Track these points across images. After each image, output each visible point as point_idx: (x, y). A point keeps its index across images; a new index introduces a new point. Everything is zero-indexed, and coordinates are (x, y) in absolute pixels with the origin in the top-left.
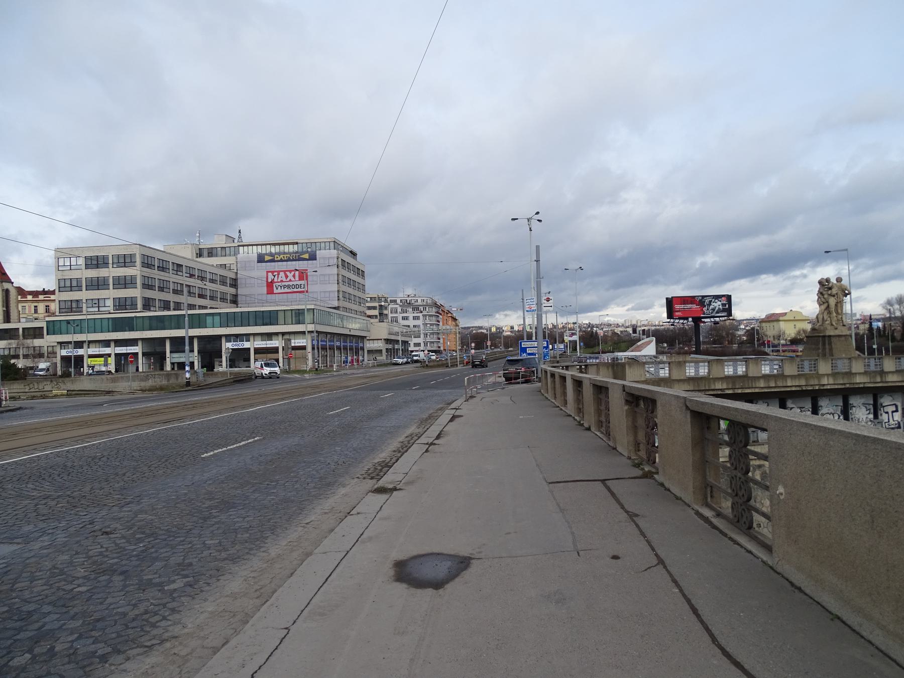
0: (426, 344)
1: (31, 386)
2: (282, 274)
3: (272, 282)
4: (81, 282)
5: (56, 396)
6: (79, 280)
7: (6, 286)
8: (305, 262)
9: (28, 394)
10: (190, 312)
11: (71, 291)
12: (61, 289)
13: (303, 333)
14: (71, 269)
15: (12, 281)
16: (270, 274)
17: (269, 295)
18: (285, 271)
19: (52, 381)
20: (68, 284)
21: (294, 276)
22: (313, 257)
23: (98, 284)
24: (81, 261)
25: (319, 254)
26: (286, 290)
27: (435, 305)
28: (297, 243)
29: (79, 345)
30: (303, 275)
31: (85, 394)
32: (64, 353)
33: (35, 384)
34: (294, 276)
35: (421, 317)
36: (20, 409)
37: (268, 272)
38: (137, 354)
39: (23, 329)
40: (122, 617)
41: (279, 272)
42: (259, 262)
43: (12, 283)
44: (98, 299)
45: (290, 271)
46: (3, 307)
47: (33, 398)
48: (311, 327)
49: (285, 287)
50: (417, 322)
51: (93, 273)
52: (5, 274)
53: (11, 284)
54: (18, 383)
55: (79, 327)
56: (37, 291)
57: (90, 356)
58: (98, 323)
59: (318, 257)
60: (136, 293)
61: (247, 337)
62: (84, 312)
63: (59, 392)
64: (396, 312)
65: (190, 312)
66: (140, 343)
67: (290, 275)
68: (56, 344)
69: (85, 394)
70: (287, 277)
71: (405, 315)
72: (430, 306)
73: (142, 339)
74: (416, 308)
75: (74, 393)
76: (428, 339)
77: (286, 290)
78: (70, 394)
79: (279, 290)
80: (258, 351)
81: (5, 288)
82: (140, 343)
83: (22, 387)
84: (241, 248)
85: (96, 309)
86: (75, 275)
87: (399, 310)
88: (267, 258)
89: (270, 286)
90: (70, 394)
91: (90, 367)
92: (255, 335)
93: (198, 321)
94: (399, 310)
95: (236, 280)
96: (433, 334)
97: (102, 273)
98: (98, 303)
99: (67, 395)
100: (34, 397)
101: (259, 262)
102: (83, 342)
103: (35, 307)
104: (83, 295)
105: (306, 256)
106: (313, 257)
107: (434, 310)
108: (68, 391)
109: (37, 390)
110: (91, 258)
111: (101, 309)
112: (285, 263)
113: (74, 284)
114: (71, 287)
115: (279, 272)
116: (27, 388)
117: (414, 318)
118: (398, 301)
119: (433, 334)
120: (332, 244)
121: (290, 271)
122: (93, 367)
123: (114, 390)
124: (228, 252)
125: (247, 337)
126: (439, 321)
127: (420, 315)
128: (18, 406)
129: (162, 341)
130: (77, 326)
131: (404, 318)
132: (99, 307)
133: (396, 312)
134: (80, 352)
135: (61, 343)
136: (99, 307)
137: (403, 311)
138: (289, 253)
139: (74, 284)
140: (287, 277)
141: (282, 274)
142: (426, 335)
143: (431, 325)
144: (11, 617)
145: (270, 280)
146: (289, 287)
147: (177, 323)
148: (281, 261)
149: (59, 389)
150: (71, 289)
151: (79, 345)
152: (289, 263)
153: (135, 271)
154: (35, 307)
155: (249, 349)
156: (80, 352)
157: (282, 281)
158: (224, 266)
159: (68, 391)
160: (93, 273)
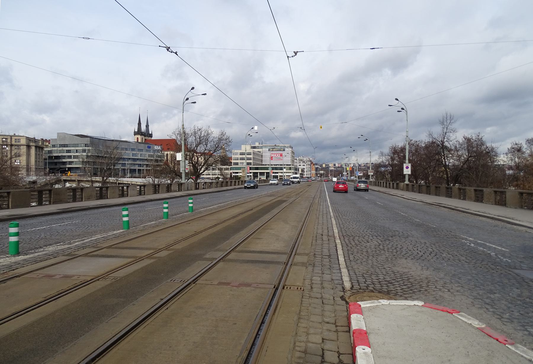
0: (307, 174)
2: (275, 155)
3: (273, 156)
6: (238, 158)
8: (282, 151)
10: (271, 166)
13: (291, 172)
16: (272, 154)
17: (271, 160)
18: (276, 154)
20: (235, 159)
21: (279, 155)
22: (284, 150)
23: (242, 159)
25: (286, 149)
26: (276, 159)
27: (311, 161)
28: (279, 146)
30: (281, 155)
34: (279, 155)
35: (306, 165)
37: (271, 154)
38: (251, 176)
41: (274, 154)
42: (269, 151)
45: (278, 154)
48: (293, 171)
49: (277, 158)
50: (304, 167)
55: (237, 169)
59: (285, 150)
60: (251, 161)
61: (278, 173)
64: (297, 163)
65: (271, 166)
66: (252, 173)
67: (278, 155)
70: (276, 155)
71: (300, 164)
72: (309, 161)
73: (253, 172)
74: (304, 162)
76: (307, 173)
77: (276, 159)
79: (274, 159)
80: (280, 176)
82: (252, 173)
84: (263, 147)
87: (298, 162)
88: (271, 150)
89: (272, 158)
92: (279, 172)
93: (267, 169)
94: (298, 162)
95: (262, 156)
96: (309, 171)
97: (244, 156)
98: (242, 163)
101: (269, 151)
104: (239, 161)
105: (282, 150)
106: (284, 150)
107: (310, 163)
110: (241, 153)
112: (276, 152)
113: (237, 159)
115: (274, 154)
117: (303, 165)
118: (298, 159)
119: (309, 171)
120: (289, 147)
121: (278, 154)
124: (259, 148)
125: (278, 173)
126: (311, 167)
127: (305, 164)
129: (257, 173)
131: (299, 165)
133: (297, 163)
134: (237, 174)
137: (299, 163)
138: (278, 149)
140: (276, 155)
141: (275, 155)
142: (307, 172)
143: (309, 168)
145: (272, 156)
146: (277, 158)
147: (262, 169)
148: (275, 151)
150: (236, 160)
152: (277, 151)
153: (251, 156)
155: (278, 176)
156: (237, 174)
157: (275, 157)
158: (258, 151)
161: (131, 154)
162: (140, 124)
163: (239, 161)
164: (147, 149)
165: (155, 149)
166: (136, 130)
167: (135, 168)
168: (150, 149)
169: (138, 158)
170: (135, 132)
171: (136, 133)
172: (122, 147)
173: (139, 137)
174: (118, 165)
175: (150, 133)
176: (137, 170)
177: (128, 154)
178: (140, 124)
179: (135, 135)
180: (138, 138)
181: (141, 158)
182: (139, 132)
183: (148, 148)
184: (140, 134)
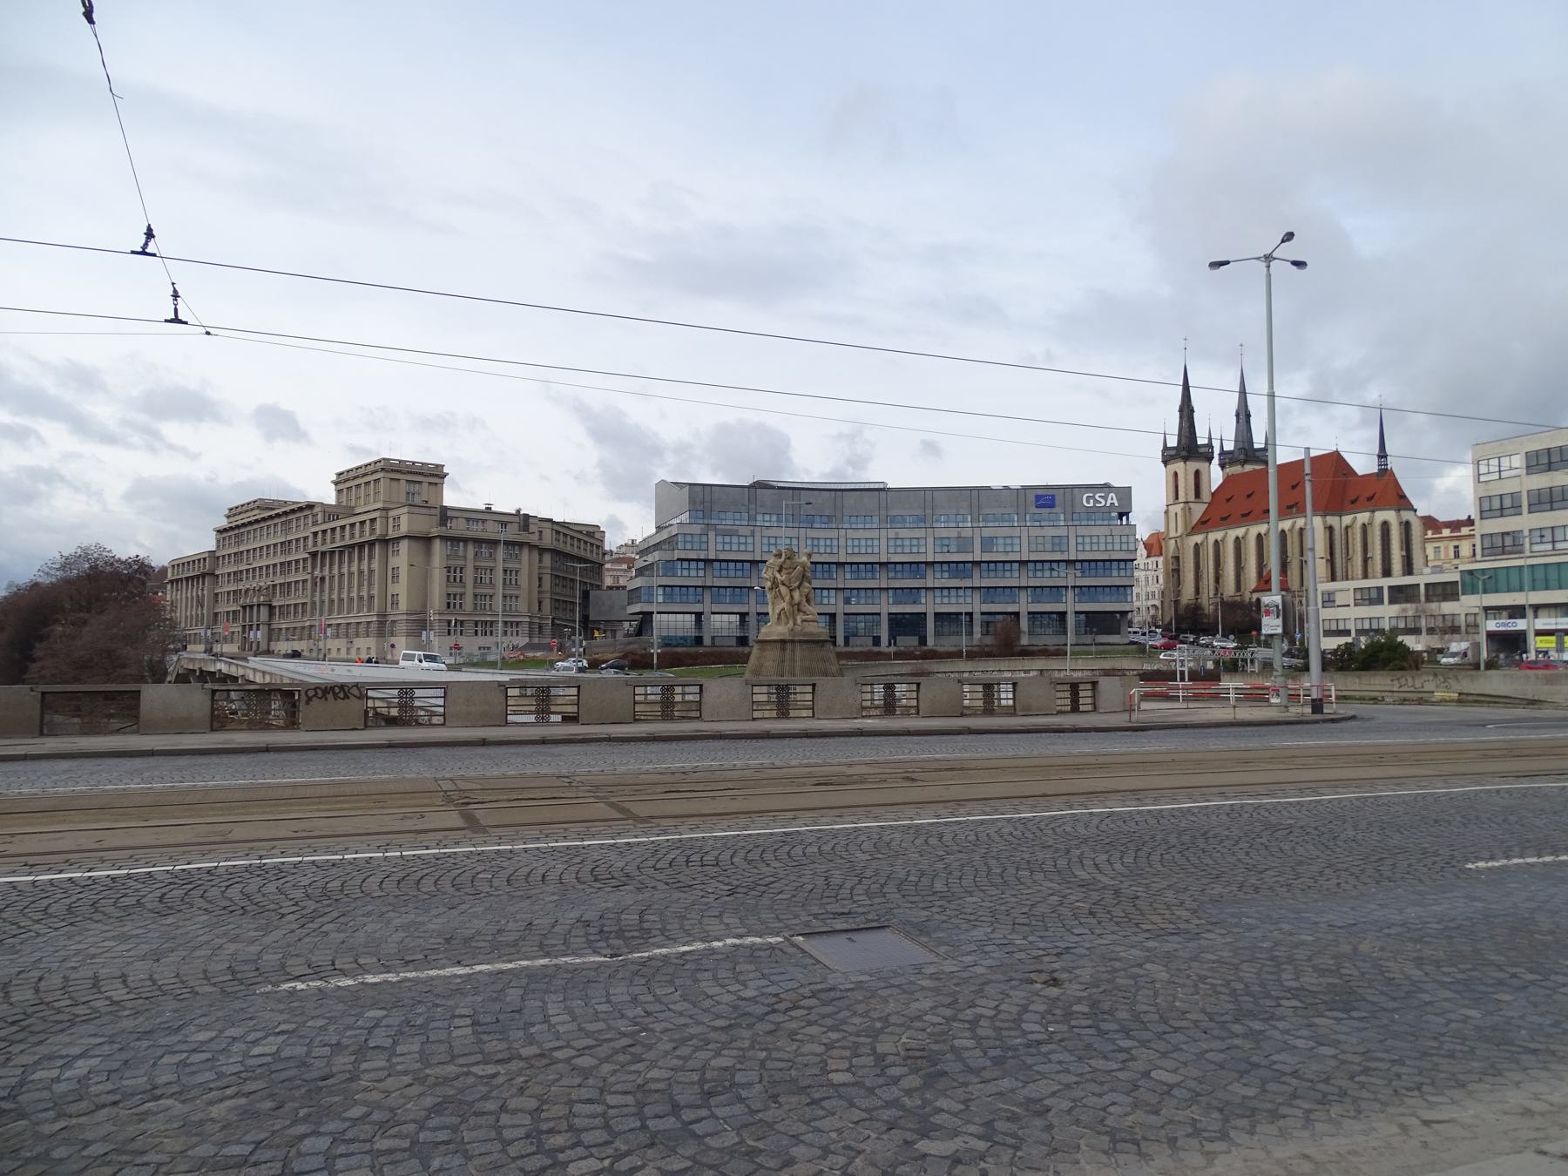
1: (1403, 681)
4: (1520, 498)
5: (1442, 702)
7: (1406, 515)
9: (1395, 694)
11: (1502, 516)
12: (1485, 515)
14: (1500, 478)
15: (1415, 507)
19: (1436, 675)
20: (1496, 504)
24: (1518, 461)
29: (1517, 612)
31: (1490, 702)
32: (1492, 625)
33: (1410, 680)
36: (1353, 718)
39: (1427, 585)
40: (1248, 1113)
43: (1416, 511)
44: (1553, 528)
46: (1402, 549)
47: (1404, 701)
51: (1541, 481)
52: (1403, 497)
53: (1412, 513)
54: (1382, 675)
56: (1458, 521)
57: (1539, 633)
58: (1502, 576)
62: (1528, 553)
63: (1447, 695)
68: (1476, 611)
69: (1490, 702)
75: (1470, 698)
78: (1463, 699)
81: (1404, 519)
83: (1389, 682)
85: (1549, 547)
86: (1509, 487)
90: (1463, 699)
91: (1541, 652)
99: (1459, 701)
100: (1405, 700)
102: (1523, 608)
103: (1456, 547)
104: (1524, 522)
108: (1460, 694)
109: (1412, 689)
111: (1559, 546)
113: (1507, 502)
114: (1502, 509)
116: (1396, 682)
122: (1546, 653)
123: (1542, 699)
128: (1351, 713)
130: (1490, 578)
132: (1554, 542)
134: (1521, 624)
135: (1486, 609)
136: (1554, 542)
139: (1507, 502)
144: (1149, 1041)
149: (1448, 689)
150: (1502, 512)
151: (1517, 612)
154: (1456, 547)
156: (1521, 624)
159: (1460, 694)
160: (1541, 481)
161: (930, 541)
162: (1187, 410)
163: (1524, 522)
164: (1033, 509)
165: (1084, 509)
166: (1173, 442)
167: (1060, 608)
168: (1054, 510)
169: (969, 558)
170: (1165, 448)
171: (1173, 452)
172: (893, 513)
173: (1179, 466)
174: (873, 597)
175: (1259, 442)
176: (977, 618)
177: (915, 542)
178: (1187, 410)
179: (1165, 462)
180: (1176, 474)
181: (986, 557)
182: (1187, 449)
183: (1037, 507)
184: (1184, 453)
